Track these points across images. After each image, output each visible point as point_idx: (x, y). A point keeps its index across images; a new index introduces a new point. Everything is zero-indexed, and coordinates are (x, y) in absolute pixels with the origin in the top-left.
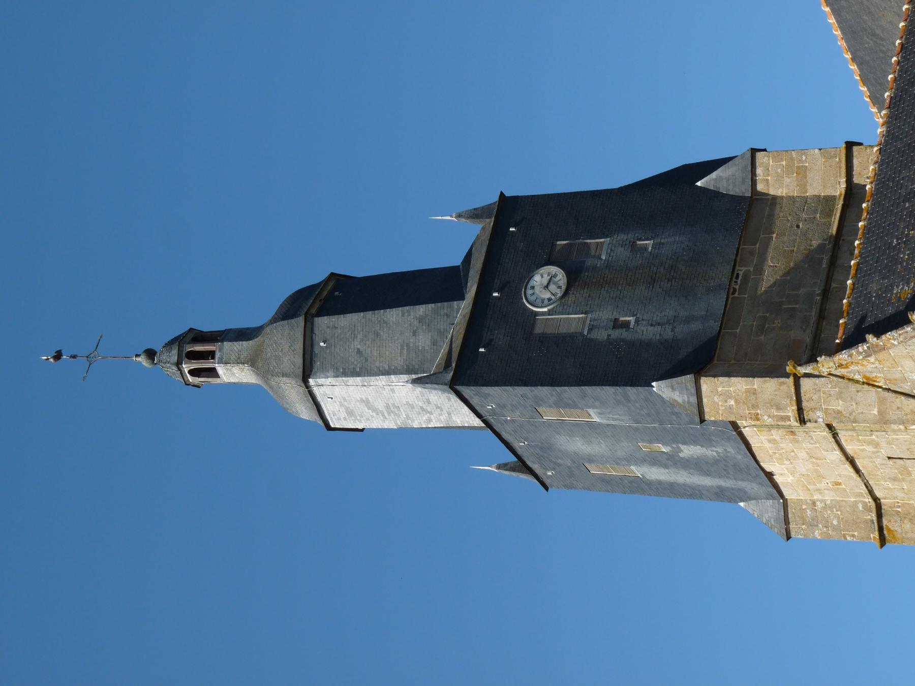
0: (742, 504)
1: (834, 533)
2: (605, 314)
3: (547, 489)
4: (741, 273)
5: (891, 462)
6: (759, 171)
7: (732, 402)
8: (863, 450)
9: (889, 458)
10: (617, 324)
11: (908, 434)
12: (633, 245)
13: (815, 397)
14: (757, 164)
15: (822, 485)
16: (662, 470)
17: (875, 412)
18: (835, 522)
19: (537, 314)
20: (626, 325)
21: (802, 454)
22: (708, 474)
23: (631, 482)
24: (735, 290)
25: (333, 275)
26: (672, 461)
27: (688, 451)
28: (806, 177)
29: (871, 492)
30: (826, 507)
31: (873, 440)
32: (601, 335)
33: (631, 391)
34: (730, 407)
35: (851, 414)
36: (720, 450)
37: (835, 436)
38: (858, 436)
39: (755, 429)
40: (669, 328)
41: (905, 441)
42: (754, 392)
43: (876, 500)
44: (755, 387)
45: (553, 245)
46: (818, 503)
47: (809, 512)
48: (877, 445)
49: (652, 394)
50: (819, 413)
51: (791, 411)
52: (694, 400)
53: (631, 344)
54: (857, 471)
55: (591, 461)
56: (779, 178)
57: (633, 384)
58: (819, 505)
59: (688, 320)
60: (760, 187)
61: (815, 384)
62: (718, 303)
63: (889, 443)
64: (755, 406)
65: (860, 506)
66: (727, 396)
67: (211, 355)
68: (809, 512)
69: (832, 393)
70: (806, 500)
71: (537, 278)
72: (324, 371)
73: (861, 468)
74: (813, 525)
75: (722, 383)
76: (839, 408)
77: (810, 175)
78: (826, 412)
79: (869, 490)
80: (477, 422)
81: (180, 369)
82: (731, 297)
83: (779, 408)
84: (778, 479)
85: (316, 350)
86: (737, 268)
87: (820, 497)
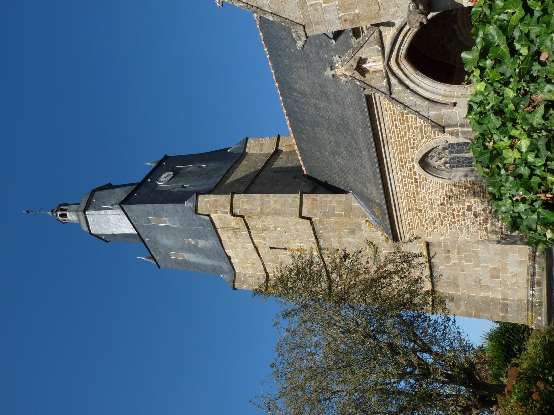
0: (222, 276)
1: (250, 287)
2: (181, 184)
3: (159, 267)
4: (230, 172)
5: (271, 250)
6: (248, 145)
7: (208, 206)
8: (260, 243)
9: (271, 248)
10: (183, 187)
11: (276, 233)
12: (199, 167)
13: (238, 203)
14: (248, 142)
15: (248, 265)
16: (194, 255)
17: (259, 209)
18: (251, 283)
19: (159, 185)
20: (186, 187)
21: (240, 246)
22: (208, 257)
23: (185, 263)
24: (226, 177)
25: (110, 183)
26: (193, 249)
27: (202, 243)
28: (263, 147)
29: (265, 268)
30: (248, 277)
31: (264, 236)
32: (176, 190)
33: (178, 206)
34: (207, 207)
35: (250, 210)
36: (211, 242)
37: (250, 233)
38: (258, 234)
39: (222, 230)
40: (199, 187)
41: (275, 237)
42: (216, 201)
43: (267, 273)
44: (217, 199)
45: (175, 167)
46: (247, 274)
47: (243, 278)
48: (265, 239)
49: (184, 206)
50: (238, 210)
51: (228, 210)
52: (195, 204)
53: (185, 192)
54: (259, 256)
55: (170, 251)
56: (254, 147)
57: (178, 203)
58: (247, 275)
59: (206, 185)
60: (247, 150)
61: (239, 197)
62: (218, 180)
63: (270, 238)
64: (216, 207)
65: (261, 276)
66: (207, 202)
67: (66, 210)
68: (243, 278)
69: (244, 201)
70: (243, 273)
71: (164, 175)
72: (91, 210)
73: (261, 254)
74: (243, 284)
75: (206, 197)
76: (246, 208)
77: (264, 146)
78: (241, 209)
79: (264, 267)
80: (134, 232)
81: (56, 214)
82: (224, 178)
83: (224, 208)
84: (233, 260)
85: (92, 202)
86: (230, 171)
87: (248, 272)
